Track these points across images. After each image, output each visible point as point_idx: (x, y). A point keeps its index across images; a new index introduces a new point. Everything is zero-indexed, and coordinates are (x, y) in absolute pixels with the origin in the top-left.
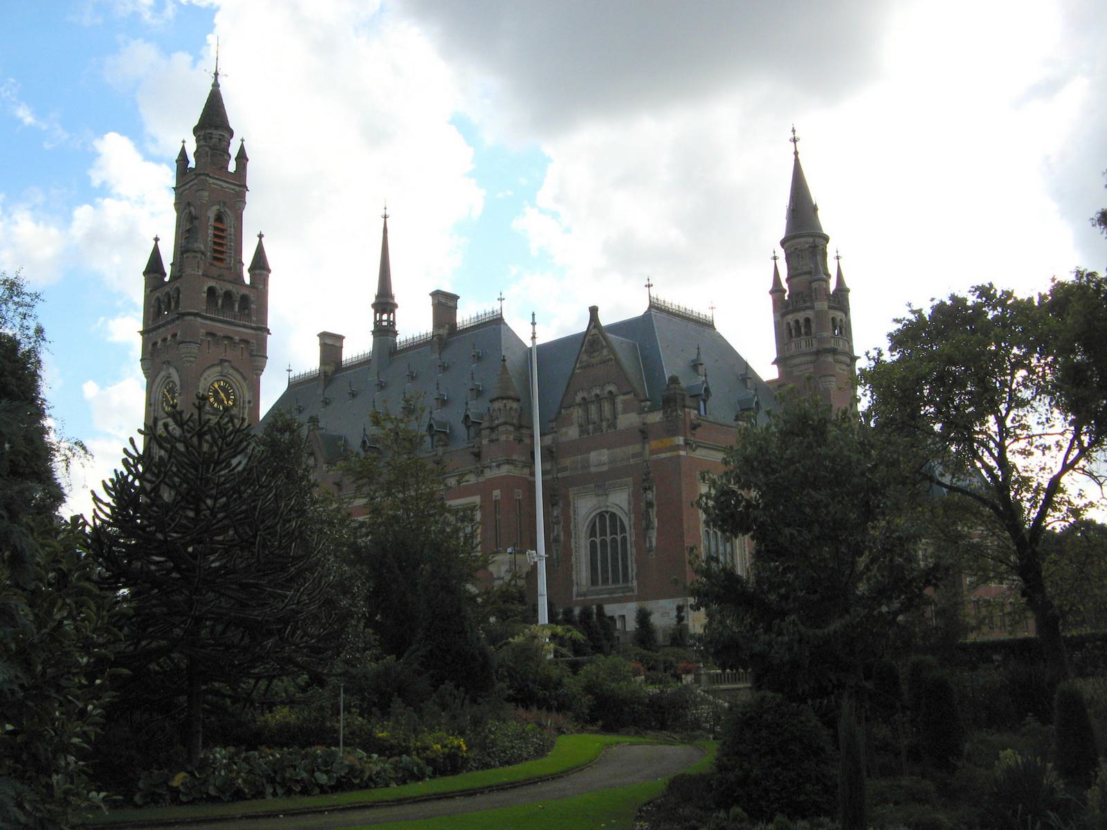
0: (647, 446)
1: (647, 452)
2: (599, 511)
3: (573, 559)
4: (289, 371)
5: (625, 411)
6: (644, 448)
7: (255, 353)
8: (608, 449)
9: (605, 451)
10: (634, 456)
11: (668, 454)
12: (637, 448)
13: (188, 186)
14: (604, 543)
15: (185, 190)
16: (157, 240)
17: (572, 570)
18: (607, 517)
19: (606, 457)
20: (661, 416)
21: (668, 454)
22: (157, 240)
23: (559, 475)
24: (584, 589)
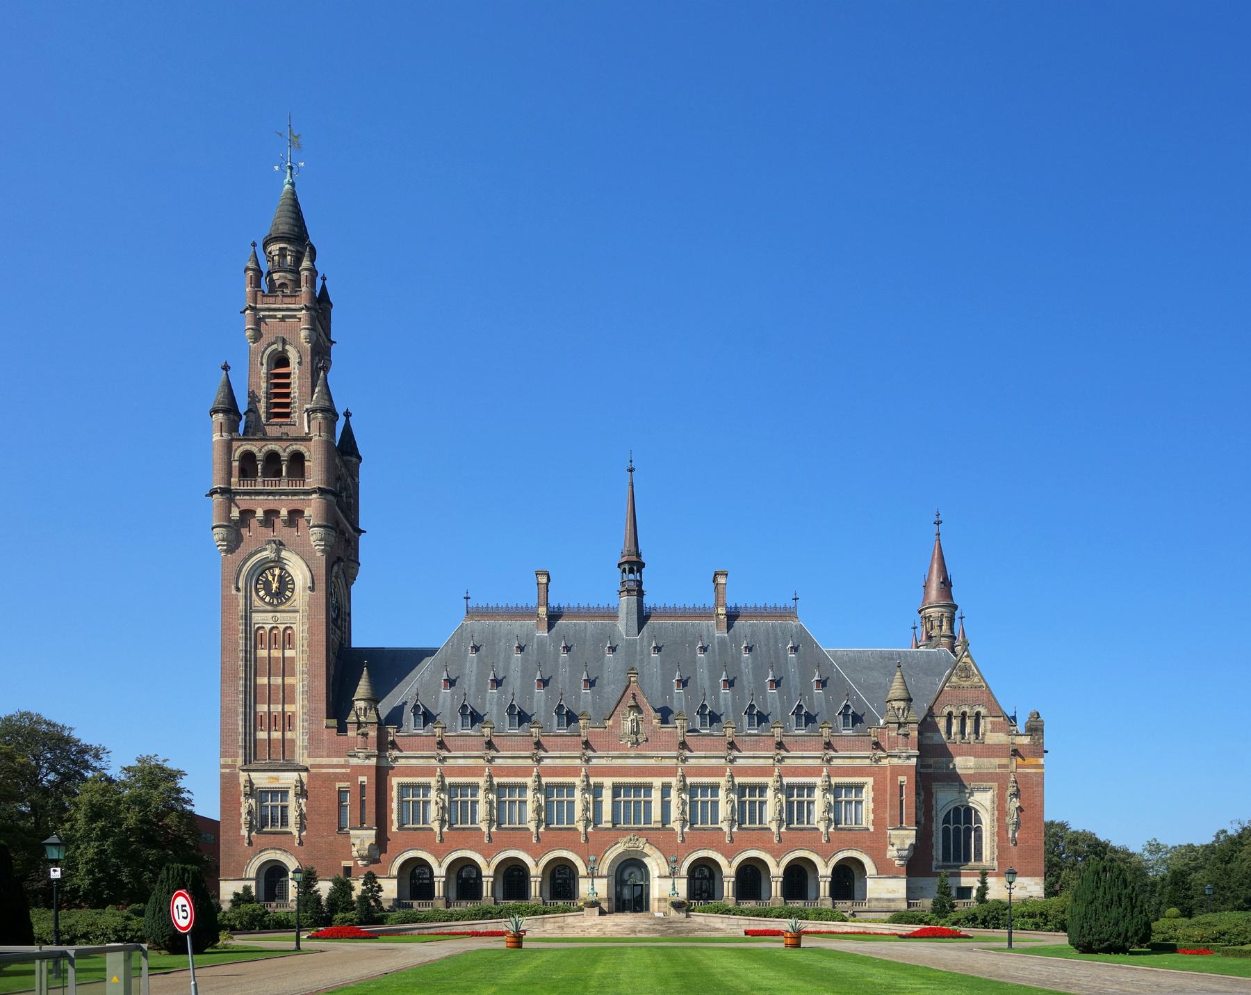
0: (1014, 761)
1: (1014, 765)
2: (959, 804)
3: (934, 839)
5: (991, 732)
6: (1011, 762)
8: (975, 757)
9: (972, 758)
10: (1000, 766)
11: (1034, 770)
12: (1005, 761)
13: (279, 314)
14: (957, 831)
15: (270, 317)
17: (933, 848)
18: (962, 810)
19: (972, 764)
20: (1029, 740)
21: (1034, 770)
23: (922, 770)
24: (941, 863)
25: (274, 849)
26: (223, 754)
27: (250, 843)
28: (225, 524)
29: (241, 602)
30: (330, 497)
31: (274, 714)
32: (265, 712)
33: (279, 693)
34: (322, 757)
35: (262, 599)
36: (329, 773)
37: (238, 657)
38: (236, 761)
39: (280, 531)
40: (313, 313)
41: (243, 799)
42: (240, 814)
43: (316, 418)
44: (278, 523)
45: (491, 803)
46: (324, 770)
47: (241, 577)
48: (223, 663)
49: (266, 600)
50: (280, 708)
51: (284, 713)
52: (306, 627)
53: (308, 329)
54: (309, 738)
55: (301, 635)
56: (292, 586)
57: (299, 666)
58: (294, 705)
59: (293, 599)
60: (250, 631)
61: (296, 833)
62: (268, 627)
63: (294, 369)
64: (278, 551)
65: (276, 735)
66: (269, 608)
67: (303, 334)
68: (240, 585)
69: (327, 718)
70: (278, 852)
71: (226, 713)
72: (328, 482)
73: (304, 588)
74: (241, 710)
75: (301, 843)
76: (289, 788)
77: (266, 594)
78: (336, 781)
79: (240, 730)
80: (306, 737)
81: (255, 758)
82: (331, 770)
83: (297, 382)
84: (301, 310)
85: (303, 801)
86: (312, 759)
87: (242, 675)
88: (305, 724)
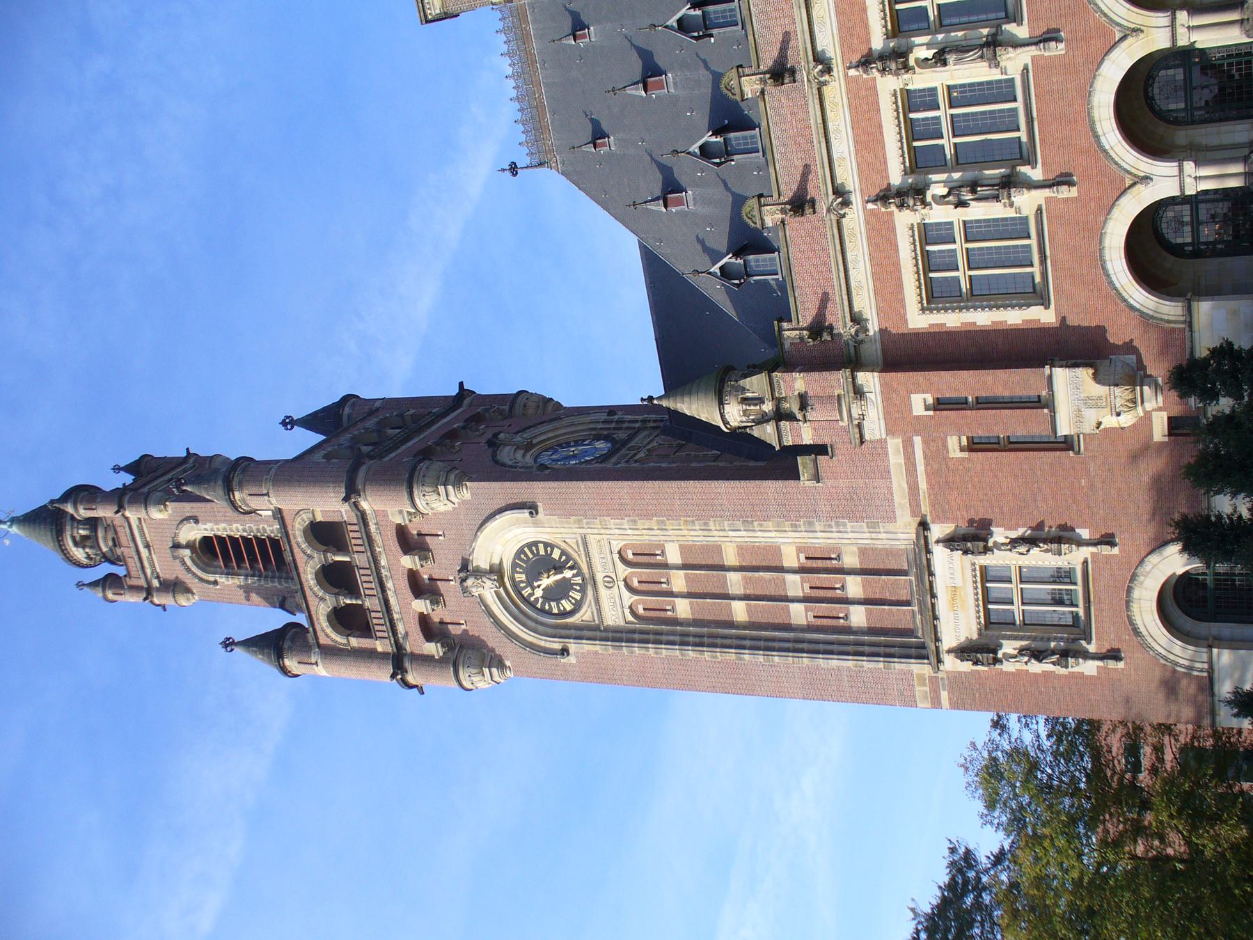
4: (514, 169)
7: (506, 408)
16: (228, 644)
22: (228, 644)
25: (1128, 603)
26: (908, 700)
27: (1114, 655)
28: (452, 669)
29: (587, 647)
30: (362, 473)
31: (807, 590)
32: (807, 610)
33: (762, 578)
34: (890, 489)
35: (578, 606)
36: (928, 474)
37: (697, 660)
38: (921, 678)
39: (441, 566)
40: (127, 498)
41: (1008, 667)
42: (1046, 674)
43: (243, 500)
44: (426, 572)
45: (940, 59)
46: (923, 485)
47: (542, 644)
48: (713, 689)
49: (578, 598)
50: (793, 579)
51: (802, 570)
52: (611, 522)
53: (146, 509)
54: (851, 519)
55: (629, 532)
56: (541, 546)
57: (696, 535)
58: (782, 547)
59: (564, 546)
60: (642, 632)
61: (1086, 552)
62: (628, 598)
63: (206, 530)
64: (478, 573)
65: (854, 587)
66: (590, 593)
67: (157, 514)
68: (558, 646)
69: (796, 477)
70: (1136, 594)
71: (815, 690)
72: (335, 481)
73: (536, 524)
74: (805, 660)
75: (1108, 540)
76: (974, 564)
77: (567, 597)
78: (946, 458)
79: (849, 663)
80: (849, 525)
81: (910, 633)
82: (921, 468)
83: (222, 525)
84: (127, 519)
85: (999, 535)
86: (898, 513)
87: (731, 655)
88: (818, 526)
